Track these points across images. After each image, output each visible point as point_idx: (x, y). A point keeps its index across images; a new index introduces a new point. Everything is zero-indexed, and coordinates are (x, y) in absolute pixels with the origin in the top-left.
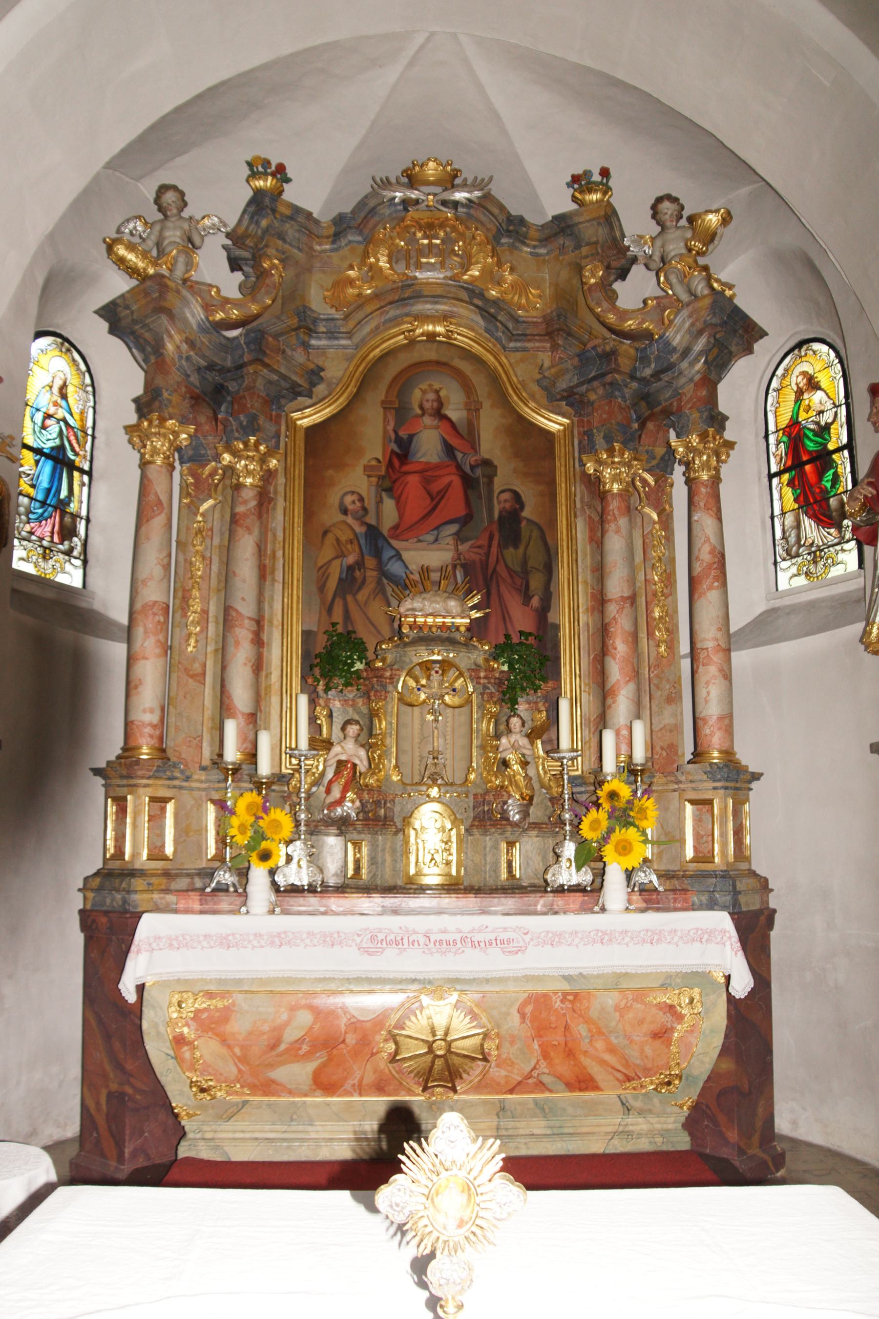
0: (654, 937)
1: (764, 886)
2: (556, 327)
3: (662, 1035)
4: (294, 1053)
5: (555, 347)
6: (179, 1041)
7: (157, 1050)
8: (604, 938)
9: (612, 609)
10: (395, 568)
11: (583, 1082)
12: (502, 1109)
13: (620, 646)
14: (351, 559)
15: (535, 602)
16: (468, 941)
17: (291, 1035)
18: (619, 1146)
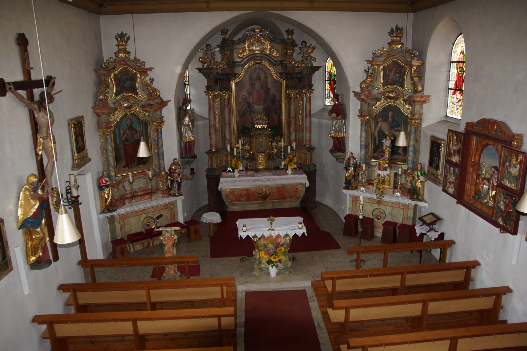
0: (295, 178)
1: (315, 166)
2: (281, 63)
3: (296, 192)
4: (243, 196)
5: (282, 65)
6: (227, 196)
7: (224, 197)
8: (288, 179)
9: (291, 119)
10: (253, 110)
11: (285, 198)
12: (273, 202)
13: (293, 126)
14: (244, 108)
15: (278, 115)
16: (268, 180)
17: (243, 194)
18: (290, 207)
